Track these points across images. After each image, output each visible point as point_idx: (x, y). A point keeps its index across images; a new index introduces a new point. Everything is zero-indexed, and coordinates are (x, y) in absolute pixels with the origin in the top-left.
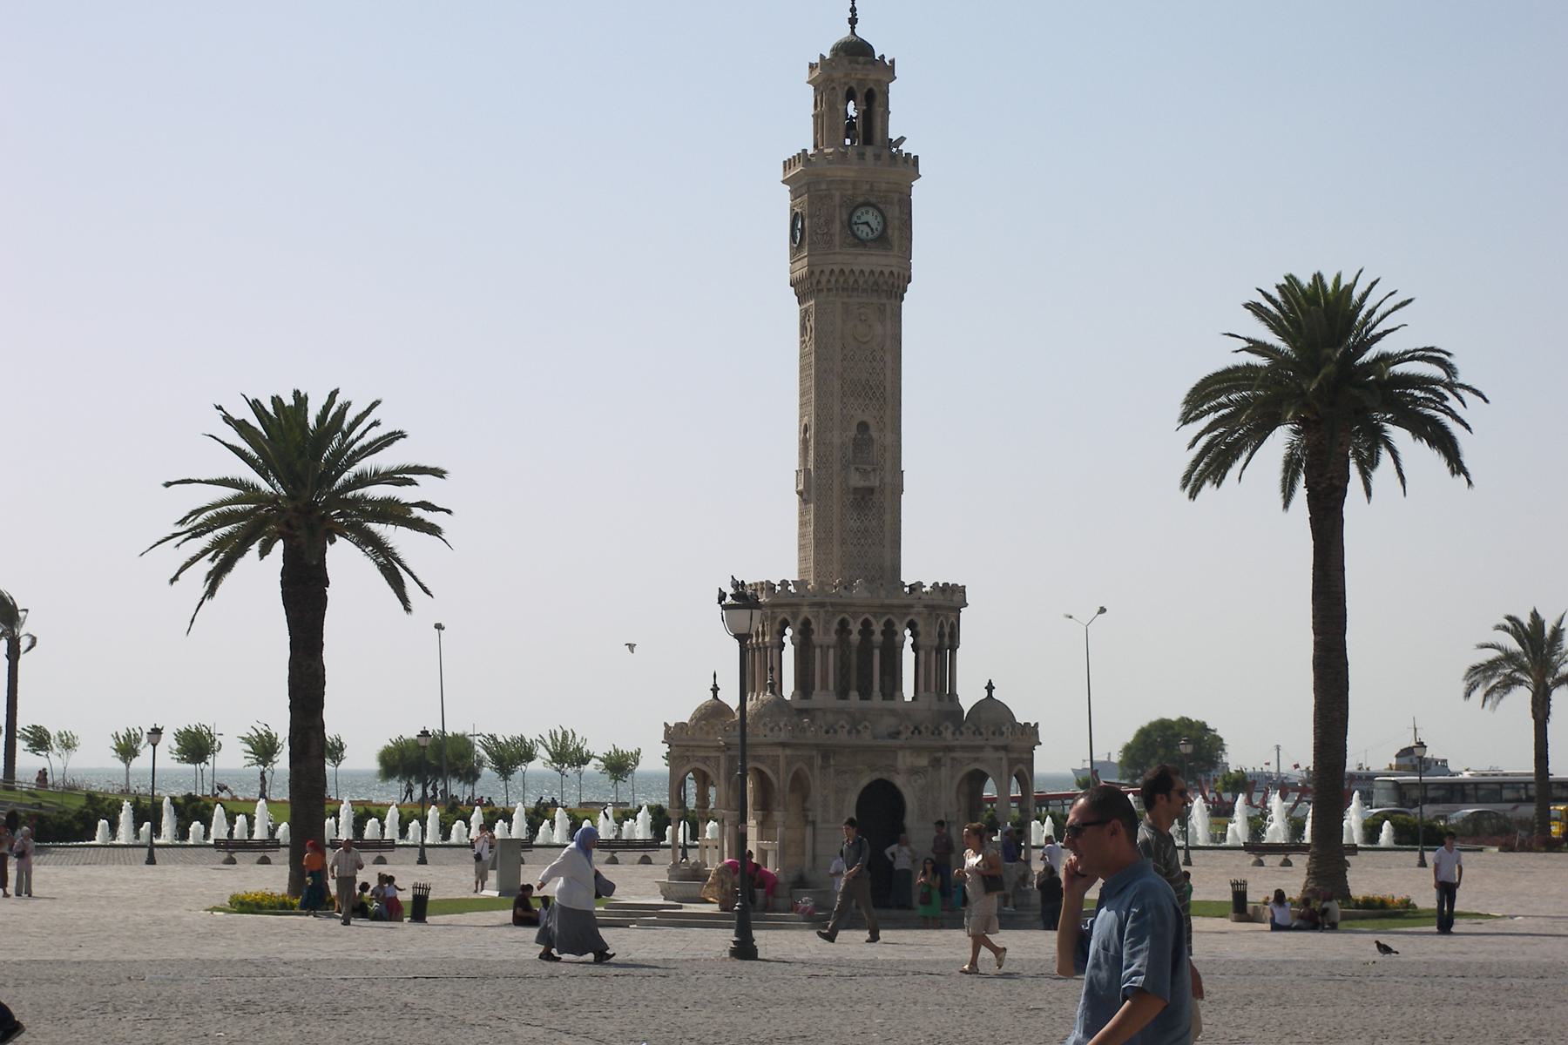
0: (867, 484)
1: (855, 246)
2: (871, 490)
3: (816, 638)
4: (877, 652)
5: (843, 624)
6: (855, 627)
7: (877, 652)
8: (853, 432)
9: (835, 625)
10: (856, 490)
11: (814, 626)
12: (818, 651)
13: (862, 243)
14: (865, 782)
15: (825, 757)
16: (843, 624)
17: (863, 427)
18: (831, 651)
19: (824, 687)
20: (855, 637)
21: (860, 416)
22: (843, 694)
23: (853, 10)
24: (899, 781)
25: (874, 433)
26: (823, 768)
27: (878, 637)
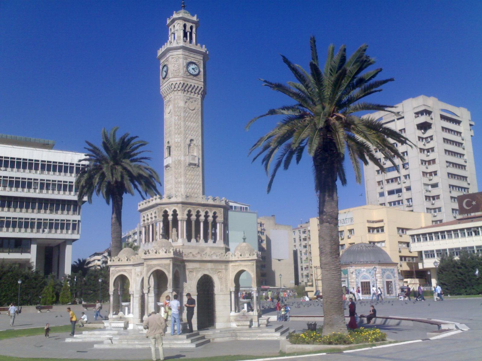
3: (179, 217)
4: (202, 225)
6: (194, 213)
7: (202, 225)
8: (188, 142)
9: (186, 212)
11: (178, 212)
12: (179, 222)
13: (191, 74)
14: (199, 276)
17: (191, 140)
18: (185, 223)
19: (182, 237)
20: (194, 217)
22: (189, 239)
27: (202, 218)
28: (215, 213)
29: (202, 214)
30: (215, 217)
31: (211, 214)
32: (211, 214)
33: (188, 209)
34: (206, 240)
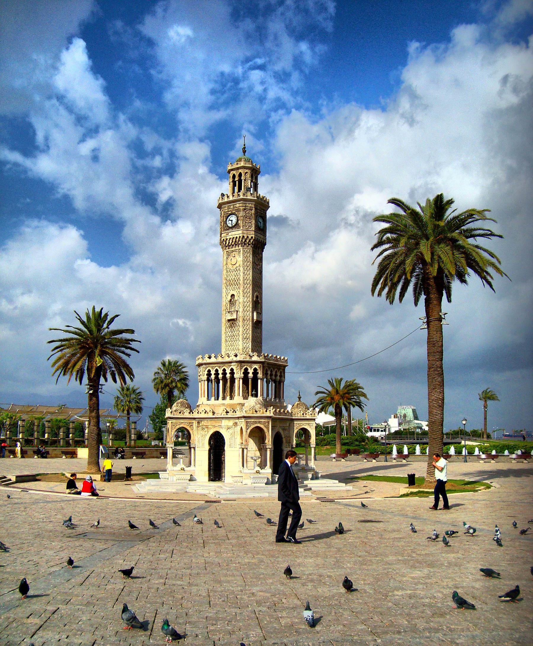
0: (232, 318)
1: (228, 230)
2: (233, 320)
4: (221, 382)
5: (209, 371)
9: (206, 372)
10: (229, 320)
14: (211, 432)
15: (198, 423)
16: (209, 371)
17: (233, 296)
21: (232, 292)
23: (244, 145)
24: (223, 432)
25: (236, 298)
26: (198, 427)
27: (220, 376)
28: (232, 370)
29: (220, 372)
30: (232, 372)
31: (228, 371)
32: (228, 371)
33: (207, 369)
34: (224, 398)
